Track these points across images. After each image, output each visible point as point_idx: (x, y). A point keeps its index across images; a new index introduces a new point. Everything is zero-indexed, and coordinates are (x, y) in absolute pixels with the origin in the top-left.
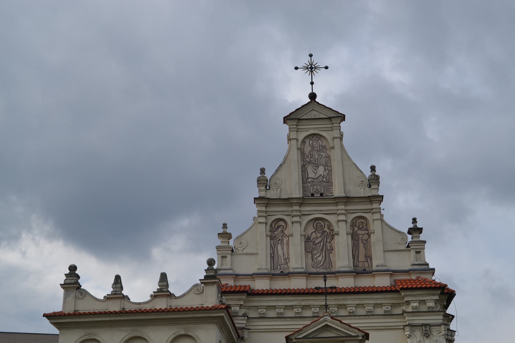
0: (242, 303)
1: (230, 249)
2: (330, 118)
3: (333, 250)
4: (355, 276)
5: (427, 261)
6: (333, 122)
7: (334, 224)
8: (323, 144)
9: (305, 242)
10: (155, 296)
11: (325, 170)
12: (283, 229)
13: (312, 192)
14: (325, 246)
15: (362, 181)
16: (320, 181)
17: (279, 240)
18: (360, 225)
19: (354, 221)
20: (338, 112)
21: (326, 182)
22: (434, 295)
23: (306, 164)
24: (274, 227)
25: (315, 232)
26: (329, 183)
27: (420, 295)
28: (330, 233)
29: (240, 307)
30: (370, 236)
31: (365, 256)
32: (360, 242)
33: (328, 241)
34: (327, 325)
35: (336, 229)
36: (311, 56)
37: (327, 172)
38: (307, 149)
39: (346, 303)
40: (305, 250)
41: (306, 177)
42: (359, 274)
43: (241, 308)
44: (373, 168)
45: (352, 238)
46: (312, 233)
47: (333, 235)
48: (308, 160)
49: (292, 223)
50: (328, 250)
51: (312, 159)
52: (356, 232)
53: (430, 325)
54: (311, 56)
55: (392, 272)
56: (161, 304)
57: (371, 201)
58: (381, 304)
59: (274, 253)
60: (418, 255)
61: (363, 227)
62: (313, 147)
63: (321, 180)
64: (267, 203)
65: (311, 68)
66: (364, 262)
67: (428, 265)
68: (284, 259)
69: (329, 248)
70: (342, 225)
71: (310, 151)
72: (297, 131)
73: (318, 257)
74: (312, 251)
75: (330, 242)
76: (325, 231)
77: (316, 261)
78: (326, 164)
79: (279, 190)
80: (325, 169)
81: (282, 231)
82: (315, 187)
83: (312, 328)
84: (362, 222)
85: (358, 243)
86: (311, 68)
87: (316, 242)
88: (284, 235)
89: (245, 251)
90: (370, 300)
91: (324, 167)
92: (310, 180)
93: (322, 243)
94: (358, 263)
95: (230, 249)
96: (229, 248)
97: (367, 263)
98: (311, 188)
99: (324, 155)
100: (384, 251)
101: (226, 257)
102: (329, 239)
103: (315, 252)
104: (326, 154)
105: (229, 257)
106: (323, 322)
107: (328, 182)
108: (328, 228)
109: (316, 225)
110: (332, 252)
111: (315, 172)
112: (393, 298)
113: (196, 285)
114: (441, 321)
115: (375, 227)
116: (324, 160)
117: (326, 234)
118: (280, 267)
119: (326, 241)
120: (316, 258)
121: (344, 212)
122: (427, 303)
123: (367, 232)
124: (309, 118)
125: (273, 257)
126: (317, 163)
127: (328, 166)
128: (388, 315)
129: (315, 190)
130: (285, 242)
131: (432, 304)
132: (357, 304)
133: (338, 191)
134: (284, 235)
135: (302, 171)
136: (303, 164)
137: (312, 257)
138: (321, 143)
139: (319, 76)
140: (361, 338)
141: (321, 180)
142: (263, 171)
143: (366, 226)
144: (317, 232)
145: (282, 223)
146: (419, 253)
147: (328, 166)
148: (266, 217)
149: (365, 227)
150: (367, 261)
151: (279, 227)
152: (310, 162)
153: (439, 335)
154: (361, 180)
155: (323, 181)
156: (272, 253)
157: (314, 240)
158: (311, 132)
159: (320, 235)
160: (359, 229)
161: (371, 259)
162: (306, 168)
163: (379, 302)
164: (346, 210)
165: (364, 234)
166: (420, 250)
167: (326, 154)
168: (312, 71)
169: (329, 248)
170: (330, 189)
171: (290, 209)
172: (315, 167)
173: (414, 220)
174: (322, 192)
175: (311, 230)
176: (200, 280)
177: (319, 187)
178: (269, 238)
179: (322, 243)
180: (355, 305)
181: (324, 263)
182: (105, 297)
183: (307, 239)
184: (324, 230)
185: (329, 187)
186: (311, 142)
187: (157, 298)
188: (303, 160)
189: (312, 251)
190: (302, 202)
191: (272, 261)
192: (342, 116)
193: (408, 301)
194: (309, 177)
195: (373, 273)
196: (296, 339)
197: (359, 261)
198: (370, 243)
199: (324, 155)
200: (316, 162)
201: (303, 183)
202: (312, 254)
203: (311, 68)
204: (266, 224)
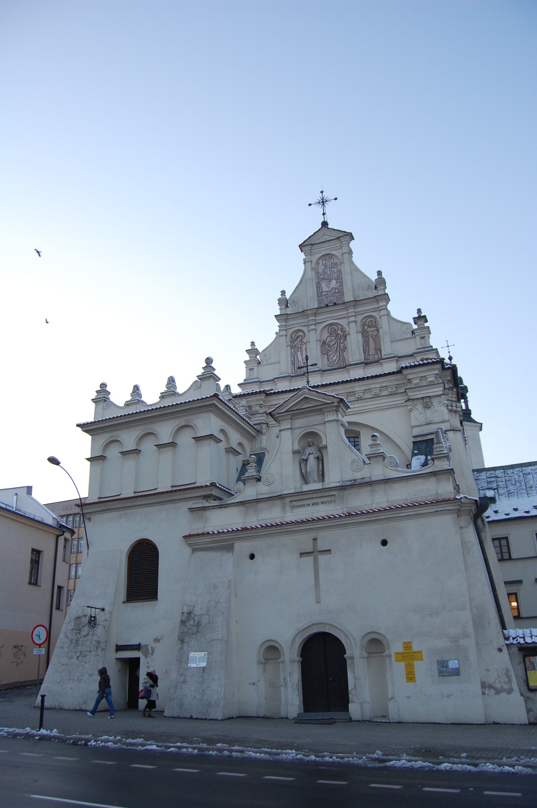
0: (262, 402)
1: (255, 362)
2: (338, 238)
3: (346, 349)
4: (364, 367)
5: (431, 344)
6: (342, 241)
7: (346, 327)
8: (334, 262)
9: (321, 346)
10: (163, 396)
12: (302, 338)
13: (326, 303)
14: (339, 347)
15: (369, 286)
16: (333, 293)
17: (298, 349)
18: (370, 323)
19: (364, 321)
20: (345, 232)
21: (339, 293)
22: (434, 370)
23: (321, 280)
24: (294, 338)
26: (341, 293)
27: (420, 372)
28: (343, 335)
29: (260, 407)
30: (379, 332)
31: (375, 349)
32: (370, 337)
33: (341, 342)
34: (305, 397)
35: (347, 329)
36: (322, 192)
37: (339, 284)
38: (321, 268)
39: (354, 390)
40: (322, 352)
41: (321, 291)
42: (368, 364)
43: (262, 408)
44: (379, 273)
45: (363, 336)
46: (327, 338)
47: (346, 336)
49: (309, 332)
50: (342, 350)
51: (325, 276)
52: (366, 330)
53: (429, 397)
54: (322, 192)
55: (397, 358)
56: (168, 402)
57: (377, 300)
58: (386, 386)
59: (294, 360)
60: (423, 340)
61: (372, 325)
62: (326, 266)
63: (334, 292)
64: (286, 319)
65: (323, 202)
66: (374, 354)
67: (432, 347)
68: (303, 364)
69: (342, 348)
70: (352, 325)
71: (324, 270)
72: (311, 255)
73: (333, 357)
74: (327, 353)
75: (343, 343)
76: (339, 334)
77: (331, 361)
78: (338, 277)
79: (297, 306)
80: (337, 282)
81: (301, 340)
82: (329, 299)
83: (291, 403)
84: (371, 321)
85: (369, 339)
87: (331, 345)
88: (303, 343)
89: (269, 362)
90: (375, 384)
91: (336, 280)
92: (324, 293)
93: (336, 344)
94: (369, 356)
95: (255, 362)
96: (255, 361)
97: (377, 355)
98: (326, 300)
99: (335, 270)
100: (392, 342)
101: (253, 369)
102: (342, 340)
103: (330, 353)
104: (338, 269)
105: (255, 368)
106: (302, 395)
107: (340, 293)
108: (341, 331)
109: (331, 330)
110: (345, 351)
111: (329, 286)
112: (398, 380)
113: (196, 381)
114: (442, 393)
115: (384, 323)
116: (336, 274)
117: (340, 336)
118: (300, 371)
119: (340, 342)
120: (332, 358)
121: (354, 314)
122: (428, 379)
123: (376, 328)
124: (321, 241)
125: (294, 363)
126: (330, 278)
127: (340, 280)
128: (392, 394)
129: (329, 301)
130: (304, 349)
131: (432, 379)
132: (364, 390)
133: (348, 297)
134: (303, 343)
135: (317, 288)
136: (317, 281)
137: (328, 358)
138: (332, 261)
139: (328, 207)
140: (337, 404)
141: (334, 292)
142: (283, 293)
143: (375, 323)
144: (331, 336)
145: (301, 333)
146: (424, 338)
147: (339, 279)
148: (286, 330)
149: (374, 325)
150: (377, 353)
151: (298, 338)
152: (323, 279)
153: (440, 405)
155: (335, 292)
156: (293, 360)
157: (329, 343)
158: (324, 253)
159: (334, 338)
160: (369, 327)
161: (381, 351)
162: (321, 285)
163: (384, 385)
164: (355, 312)
165: (373, 331)
166: (424, 335)
167: (338, 269)
168: (323, 204)
169: (342, 348)
170: (342, 298)
171: (306, 320)
172: (328, 281)
173: (419, 311)
174: (335, 301)
175: (325, 335)
176: (197, 376)
177: (332, 298)
178: (289, 348)
179: (336, 344)
180: (363, 391)
181: (338, 361)
182: (125, 404)
183: (322, 344)
184: (338, 333)
185: (341, 296)
186: (324, 262)
187: (165, 399)
188: (318, 278)
189: (327, 353)
190: (316, 311)
191: (293, 366)
192: (348, 234)
193: (410, 379)
194: (323, 291)
195: (380, 361)
196: (278, 414)
197: (370, 354)
198: (379, 337)
199: (335, 270)
200: (329, 277)
201: (318, 297)
202: (328, 355)
203: (323, 202)
204: (286, 336)
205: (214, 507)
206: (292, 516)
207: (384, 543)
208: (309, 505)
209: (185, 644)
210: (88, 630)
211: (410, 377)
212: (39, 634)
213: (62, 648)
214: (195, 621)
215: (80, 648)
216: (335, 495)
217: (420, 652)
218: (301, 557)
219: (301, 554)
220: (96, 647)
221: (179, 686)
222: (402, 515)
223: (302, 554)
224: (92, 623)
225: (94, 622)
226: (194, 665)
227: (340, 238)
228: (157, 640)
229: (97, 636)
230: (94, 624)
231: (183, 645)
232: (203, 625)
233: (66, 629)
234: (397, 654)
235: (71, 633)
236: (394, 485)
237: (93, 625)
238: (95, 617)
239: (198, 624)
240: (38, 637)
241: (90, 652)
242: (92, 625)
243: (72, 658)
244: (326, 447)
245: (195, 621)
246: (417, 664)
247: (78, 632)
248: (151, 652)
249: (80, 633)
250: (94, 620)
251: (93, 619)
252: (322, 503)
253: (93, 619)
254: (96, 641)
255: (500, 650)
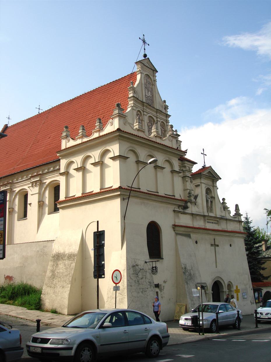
11: (151, 94)
54: (144, 35)
86: (144, 42)
87: (150, 127)
92: (146, 96)
206: (209, 226)
207: (231, 245)
208: (211, 223)
209: (189, 285)
210: (142, 275)
211: (186, 165)
212: (116, 276)
213: (131, 286)
214: (188, 273)
215: (141, 286)
216: (218, 221)
217: (239, 290)
218: (211, 246)
219: (211, 245)
220: (150, 286)
221: (193, 306)
222: (236, 235)
223: (212, 245)
224: (154, 271)
225: (156, 270)
226: (195, 295)
227: (154, 71)
228: (165, 282)
229: (148, 279)
230: (156, 271)
231: (188, 285)
232: (192, 275)
233: (129, 274)
234: (235, 290)
235: (133, 276)
236: (231, 222)
237: (155, 272)
238: (155, 267)
239: (190, 275)
240: (116, 279)
241: (147, 288)
242: (155, 272)
243: (139, 293)
244: (214, 198)
245: (188, 273)
246: (239, 294)
247: (137, 275)
248: (163, 288)
249: (138, 277)
250: (155, 269)
251: (154, 268)
253: (154, 268)
254: (149, 282)
255: (252, 289)
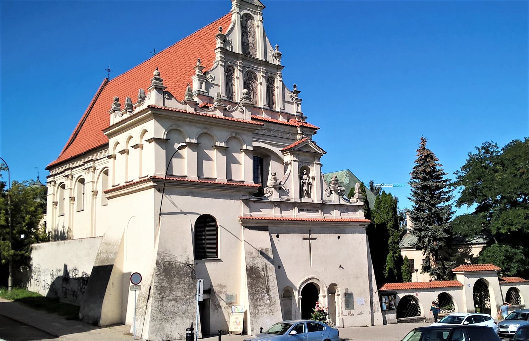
15: (273, 54)
25: (248, 79)
48: (244, 30)
92: (245, 44)
154: (272, 53)
157: (248, 84)
205: (255, 202)
219: (303, 238)
223: (304, 239)
252: (312, 210)
